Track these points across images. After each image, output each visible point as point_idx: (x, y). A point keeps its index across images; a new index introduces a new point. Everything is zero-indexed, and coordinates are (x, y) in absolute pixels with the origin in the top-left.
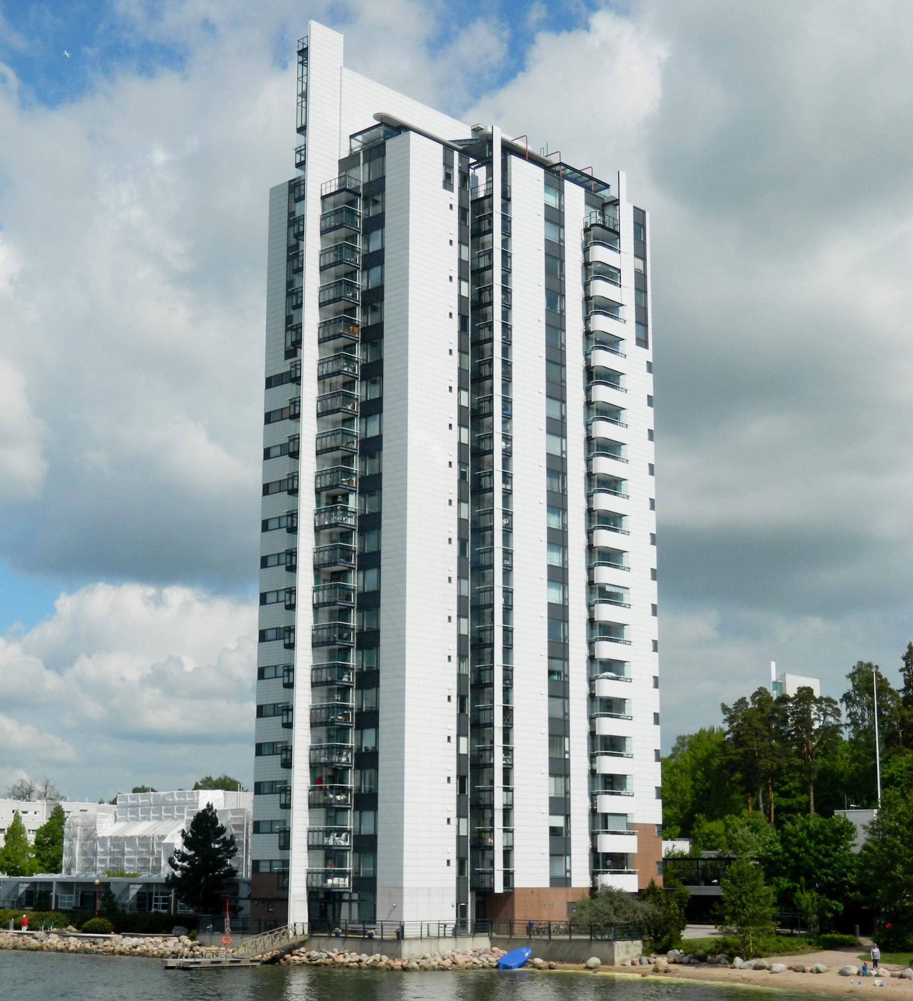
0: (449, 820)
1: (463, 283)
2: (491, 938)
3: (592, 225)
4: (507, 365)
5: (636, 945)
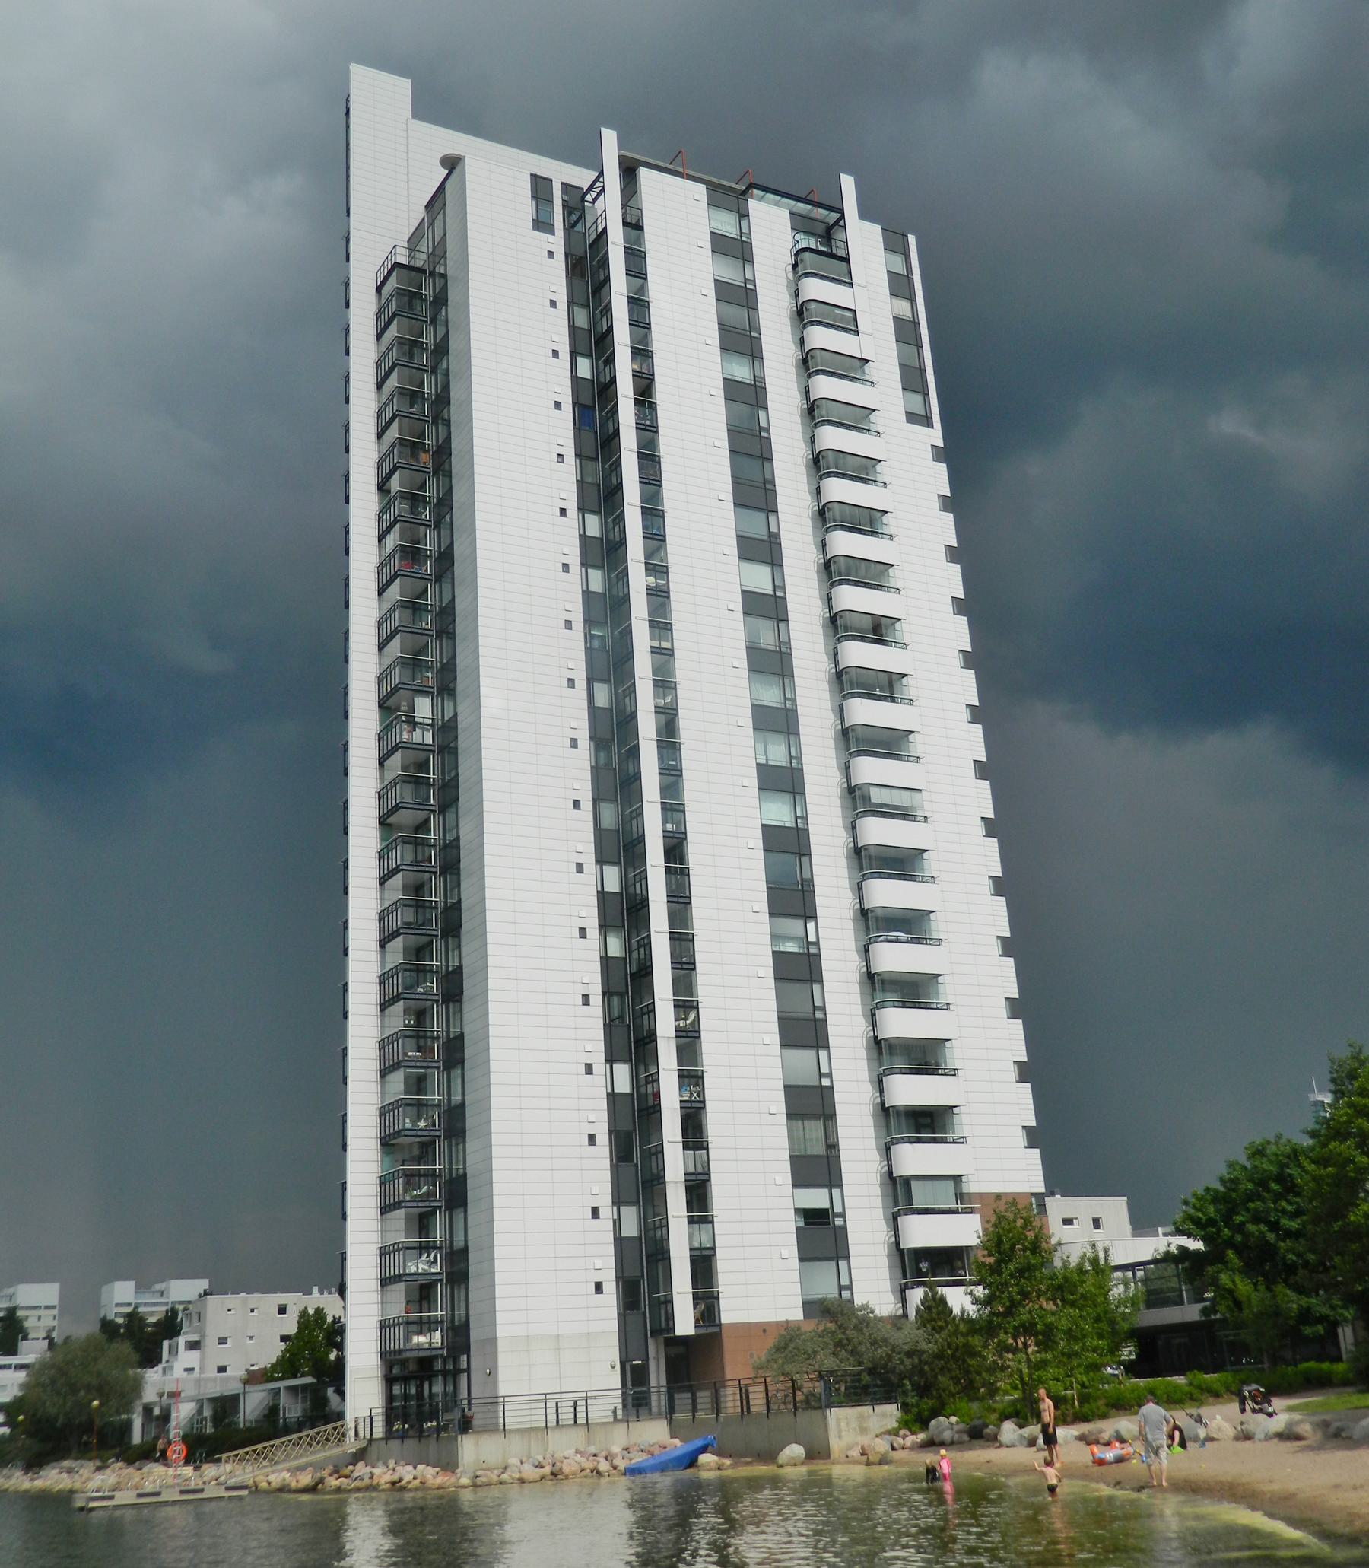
0: (595, 1213)
1: (578, 359)
2: (670, 1422)
3: (797, 254)
4: (649, 458)
5: (884, 1415)
